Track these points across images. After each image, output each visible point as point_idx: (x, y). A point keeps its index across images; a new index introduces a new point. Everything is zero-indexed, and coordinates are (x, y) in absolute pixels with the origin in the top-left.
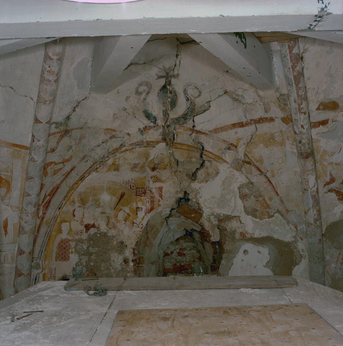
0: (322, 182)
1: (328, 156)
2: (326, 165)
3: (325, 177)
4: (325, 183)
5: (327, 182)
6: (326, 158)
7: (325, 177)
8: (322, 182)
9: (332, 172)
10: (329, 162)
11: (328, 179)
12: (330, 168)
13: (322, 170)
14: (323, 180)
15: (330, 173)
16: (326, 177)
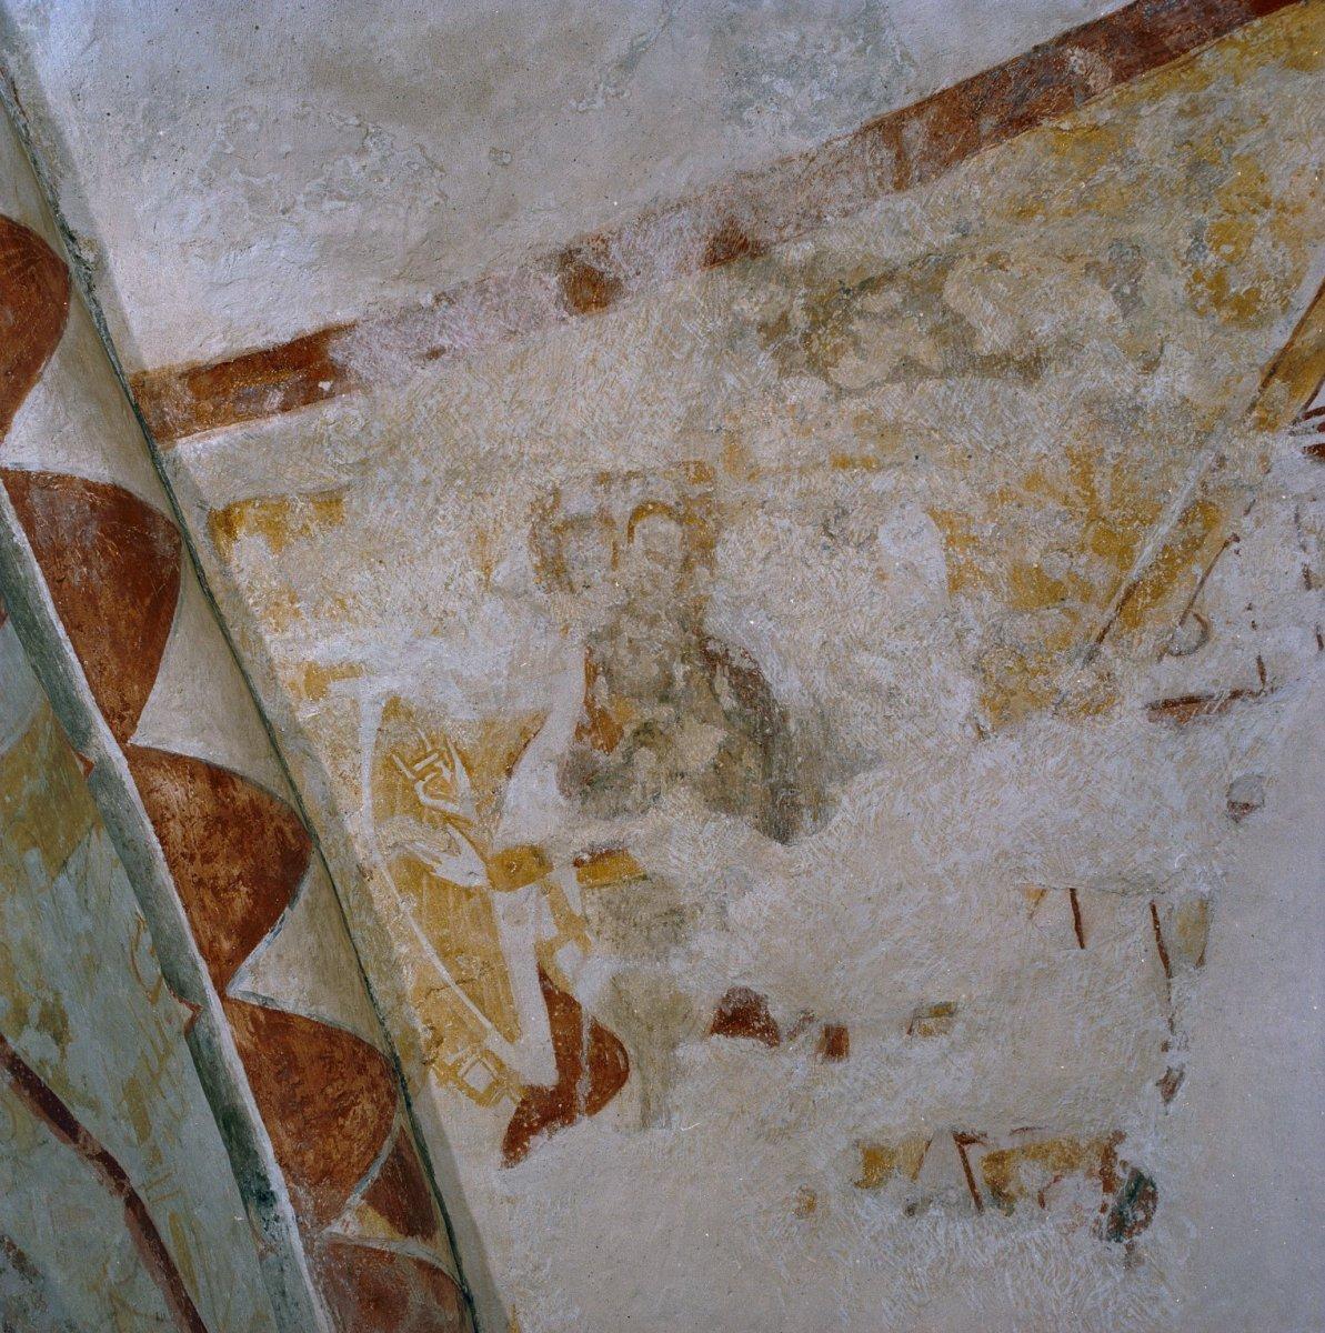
0: (471, 1093)
1: (469, 769)
2: (468, 893)
3: (494, 1041)
4: (508, 1107)
5: (534, 1092)
6: (451, 808)
7: (494, 1041)
8: (471, 1093)
9: (565, 960)
10: (497, 849)
11: (534, 1057)
12: (521, 925)
13: (444, 955)
14: (479, 1078)
15: (543, 976)
16: (510, 1038)
